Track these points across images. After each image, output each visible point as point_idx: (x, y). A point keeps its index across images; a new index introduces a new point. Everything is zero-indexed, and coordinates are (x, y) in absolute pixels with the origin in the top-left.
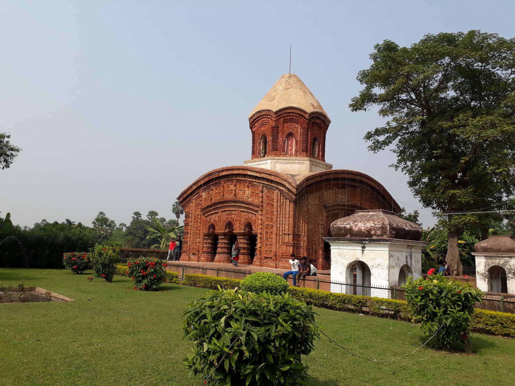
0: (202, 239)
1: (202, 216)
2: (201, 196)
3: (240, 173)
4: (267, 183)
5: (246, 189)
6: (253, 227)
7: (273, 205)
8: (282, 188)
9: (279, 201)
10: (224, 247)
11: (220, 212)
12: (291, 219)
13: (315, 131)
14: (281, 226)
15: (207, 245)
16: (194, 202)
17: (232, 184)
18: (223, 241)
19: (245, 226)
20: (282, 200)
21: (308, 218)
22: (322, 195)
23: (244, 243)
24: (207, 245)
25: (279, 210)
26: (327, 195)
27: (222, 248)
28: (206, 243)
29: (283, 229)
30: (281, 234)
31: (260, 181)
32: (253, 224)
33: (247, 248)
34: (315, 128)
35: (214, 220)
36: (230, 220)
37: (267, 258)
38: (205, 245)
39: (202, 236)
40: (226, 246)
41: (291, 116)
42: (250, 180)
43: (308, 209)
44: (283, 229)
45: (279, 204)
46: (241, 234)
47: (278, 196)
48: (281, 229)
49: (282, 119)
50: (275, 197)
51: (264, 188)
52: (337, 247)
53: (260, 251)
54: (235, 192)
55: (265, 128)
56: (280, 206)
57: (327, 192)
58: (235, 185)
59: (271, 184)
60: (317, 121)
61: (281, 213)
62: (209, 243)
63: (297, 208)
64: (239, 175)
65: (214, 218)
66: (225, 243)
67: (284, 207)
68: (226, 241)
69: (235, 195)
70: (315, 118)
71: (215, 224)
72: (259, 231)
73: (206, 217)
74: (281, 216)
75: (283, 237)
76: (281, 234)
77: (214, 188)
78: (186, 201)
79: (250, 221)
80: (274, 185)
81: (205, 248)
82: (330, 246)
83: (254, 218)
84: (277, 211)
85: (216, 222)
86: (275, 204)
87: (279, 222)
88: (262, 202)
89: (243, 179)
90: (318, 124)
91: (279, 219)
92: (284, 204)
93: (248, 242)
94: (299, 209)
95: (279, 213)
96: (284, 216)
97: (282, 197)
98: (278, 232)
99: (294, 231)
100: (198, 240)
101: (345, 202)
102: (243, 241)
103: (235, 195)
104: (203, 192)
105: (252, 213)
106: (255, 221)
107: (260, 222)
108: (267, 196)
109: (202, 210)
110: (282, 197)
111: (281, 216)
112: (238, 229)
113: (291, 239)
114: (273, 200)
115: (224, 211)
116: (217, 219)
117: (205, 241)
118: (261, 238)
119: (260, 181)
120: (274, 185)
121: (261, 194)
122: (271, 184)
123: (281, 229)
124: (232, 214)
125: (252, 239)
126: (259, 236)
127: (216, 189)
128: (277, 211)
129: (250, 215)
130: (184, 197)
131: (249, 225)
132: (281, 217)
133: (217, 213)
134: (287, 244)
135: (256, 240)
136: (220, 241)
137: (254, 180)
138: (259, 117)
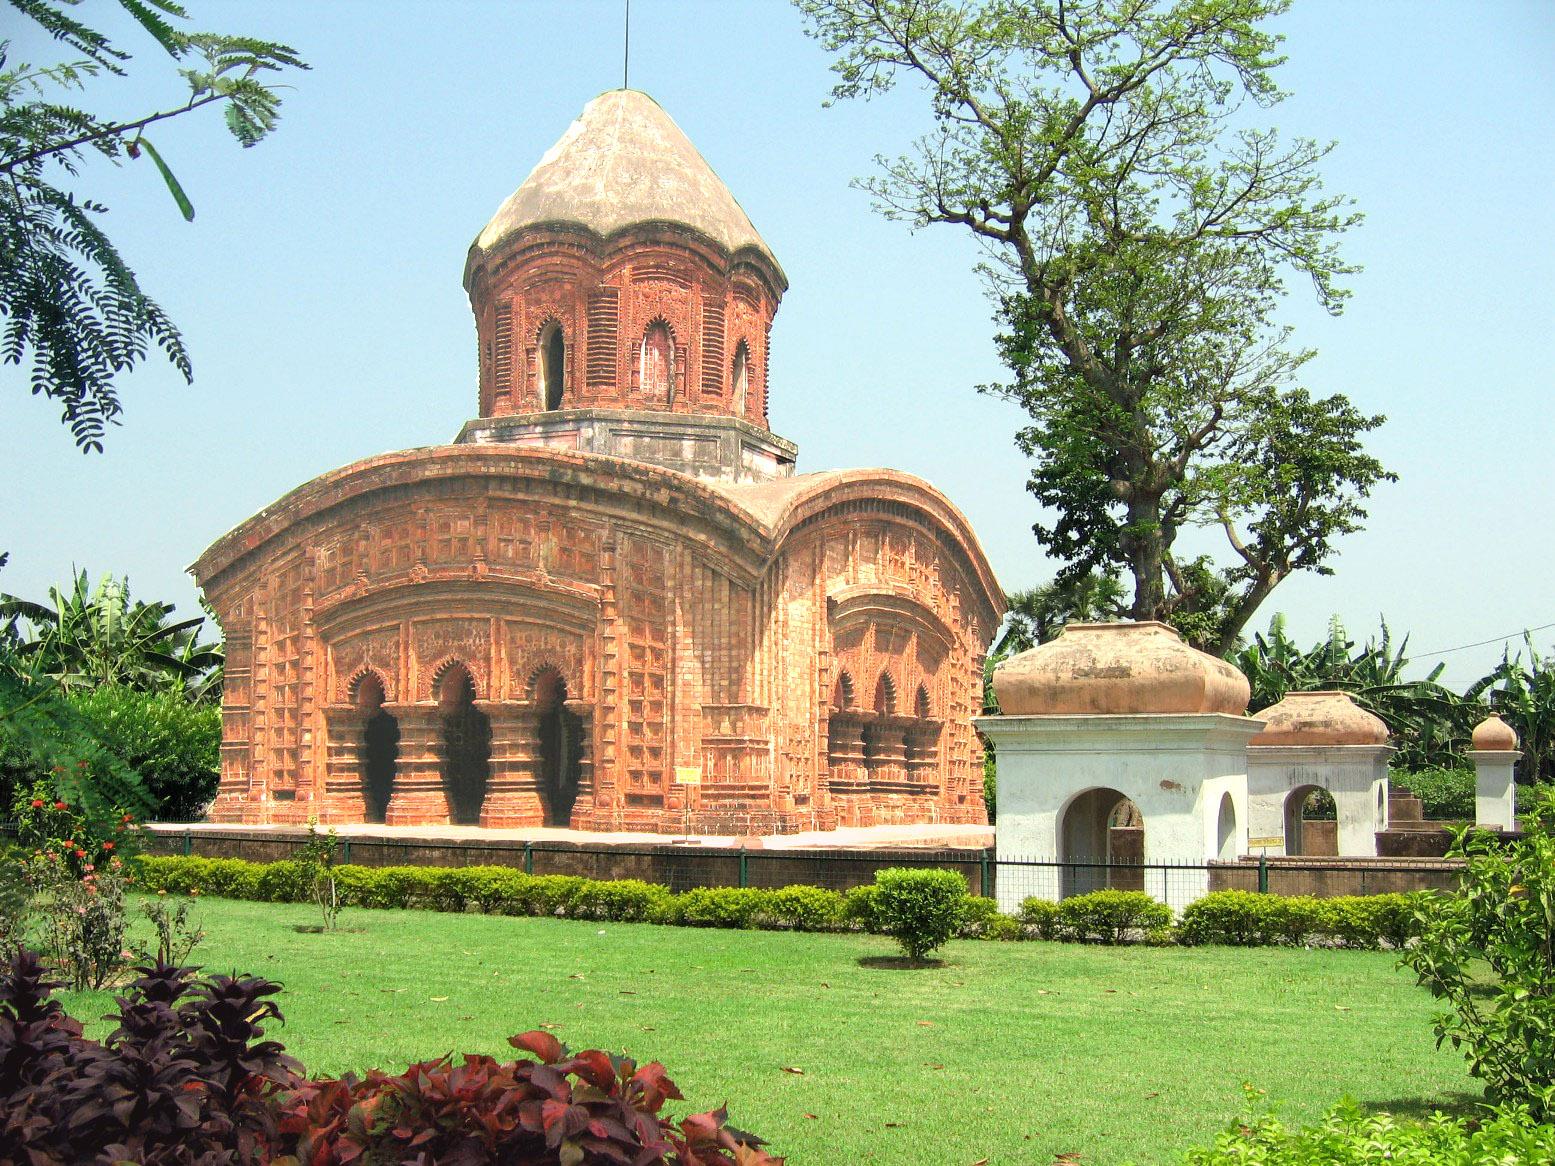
4: (634, 516)
16: (274, 581)
31: (601, 508)
32: (566, 673)
41: (659, 255)
42: (557, 501)
46: (513, 713)
49: (629, 267)
63: (758, 613)
64: (502, 479)
77: (374, 530)
79: (551, 661)
89: (521, 496)
104: (317, 544)
105: (562, 630)
127: (388, 534)
129: (554, 640)
133: (397, 628)
137: (573, 503)
138: (531, 248)
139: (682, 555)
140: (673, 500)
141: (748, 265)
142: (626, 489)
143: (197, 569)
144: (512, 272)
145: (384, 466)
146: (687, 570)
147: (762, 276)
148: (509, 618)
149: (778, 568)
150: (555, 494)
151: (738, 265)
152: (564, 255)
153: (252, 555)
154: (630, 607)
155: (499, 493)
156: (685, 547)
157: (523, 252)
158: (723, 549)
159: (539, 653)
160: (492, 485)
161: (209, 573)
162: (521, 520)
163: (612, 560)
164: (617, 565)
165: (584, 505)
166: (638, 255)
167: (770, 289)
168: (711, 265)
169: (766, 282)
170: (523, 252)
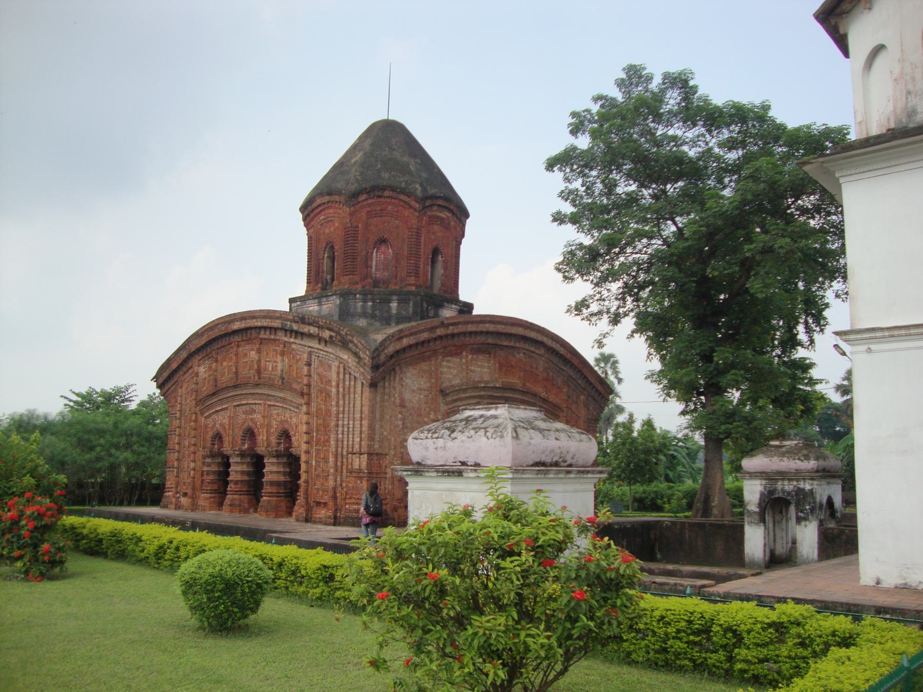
0: (199, 464)
2: (197, 374)
3: (265, 324)
4: (317, 346)
5: (279, 358)
6: (293, 439)
7: (328, 395)
8: (345, 357)
9: (341, 385)
12: (365, 423)
13: (434, 233)
14: (346, 436)
15: (211, 477)
17: (252, 350)
18: (239, 468)
20: (347, 383)
21: (403, 419)
22: (437, 369)
23: (278, 472)
25: (341, 402)
26: (449, 367)
27: (236, 483)
28: (208, 473)
29: (350, 443)
30: (345, 453)
32: (292, 433)
34: (436, 228)
35: (221, 425)
36: (251, 424)
37: (318, 504)
40: (246, 478)
42: (286, 339)
43: (402, 400)
44: (350, 443)
45: (341, 390)
47: (338, 373)
48: (345, 443)
50: (334, 376)
51: (313, 357)
52: (420, 485)
54: (259, 366)
55: (332, 229)
56: (344, 396)
57: (448, 361)
58: (259, 351)
59: (326, 349)
60: (439, 214)
61: (347, 409)
62: (214, 473)
63: (378, 399)
64: (265, 328)
65: (221, 419)
66: (243, 473)
67: (352, 396)
68: (245, 468)
69: (259, 372)
70: (435, 208)
71: (222, 432)
72: (304, 447)
74: (346, 416)
75: (350, 461)
76: (345, 453)
78: (169, 385)
79: (286, 426)
80: (330, 350)
82: (406, 484)
83: (294, 420)
84: (338, 405)
85: (225, 429)
86: (334, 390)
87: (340, 429)
88: (309, 386)
90: (442, 219)
91: (340, 423)
92: (352, 390)
94: (382, 401)
95: (341, 409)
96: (351, 415)
97: (347, 376)
98: (340, 450)
99: (369, 446)
101: (487, 382)
102: (275, 469)
103: (259, 372)
104: (199, 366)
107: (304, 428)
108: (318, 374)
109: (198, 402)
110: (347, 376)
111: (346, 416)
112: (265, 442)
113: (365, 463)
114: (330, 381)
115: (238, 406)
116: (226, 421)
117: (205, 469)
118: (307, 462)
119: (303, 343)
120: (330, 350)
121: (306, 368)
122: (326, 349)
123: (345, 443)
124: (254, 411)
125: (292, 462)
126: (303, 458)
128: (338, 405)
130: (165, 375)
131: (286, 435)
132: (346, 419)
133: (227, 409)
134: (357, 474)
136: (232, 468)
137: (292, 340)
138: (320, 205)
139: (339, 367)
140: (331, 337)
141: (439, 205)
142: (312, 332)
143: (156, 378)
144: (313, 219)
145: (218, 324)
146: (341, 376)
147: (450, 211)
149: (395, 373)
150: (286, 336)
151: (431, 206)
152: (335, 208)
153: (175, 371)
154: (317, 398)
155: (264, 336)
156: (340, 363)
157: (316, 208)
158: (355, 364)
159: (281, 422)
160: (262, 332)
161: (161, 380)
162: (275, 350)
163: (309, 371)
164: (312, 373)
165: (297, 341)
166: (370, 205)
167: (457, 217)
168: (411, 207)
169: (453, 213)
170: (316, 208)
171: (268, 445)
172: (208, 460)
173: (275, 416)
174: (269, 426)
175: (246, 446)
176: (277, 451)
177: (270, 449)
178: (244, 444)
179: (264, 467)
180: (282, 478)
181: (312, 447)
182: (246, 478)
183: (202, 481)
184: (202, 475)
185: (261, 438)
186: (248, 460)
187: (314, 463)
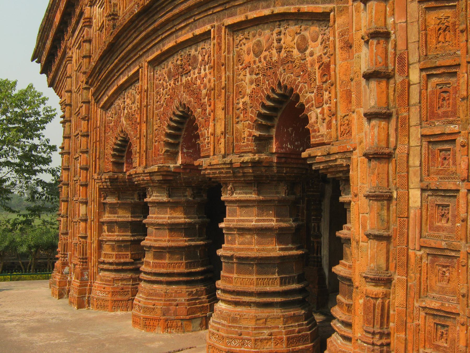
0: (94, 207)
1: (93, 107)
6: (314, 115)
10: (172, 251)
11: (146, 73)
15: (117, 235)
19: (266, 120)
23: (261, 232)
24: (117, 235)
27: (160, 252)
28: (111, 224)
32: (307, 96)
33: (281, 263)
36: (186, 98)
38: (106, 235)
39: (94, 188)
40: (182, 241)
53: (380, 315)
66: (173, 228)
68: (179, 217)
72: (367, 135)
73: (106, 107)
81: (106, 250)
83: (316, 49)
93: (289, 223)
100: (83, 209)
102: (252, 219)
106: (326, 69)
117: (107, 217)
118: (382, 198)
126: (362, 179)
131: (285, 113)
135: (340, 215)
143: (36, 56)
148: (229, 21)
171: (231, 148)
172: (110, 200)
173: (248, 58)
174: (230, 91)
175: (179, 162)
176: (255, 164)
177: (236, 159)
178: (173, 156)
179: (221, 215)
180: (274, 249)
181: (404, 126)
182: (182, 241)
183: (100, 244)
184: (100, 231)
185: (212, 131)
186: (188, 196)
187: (415, 195)
